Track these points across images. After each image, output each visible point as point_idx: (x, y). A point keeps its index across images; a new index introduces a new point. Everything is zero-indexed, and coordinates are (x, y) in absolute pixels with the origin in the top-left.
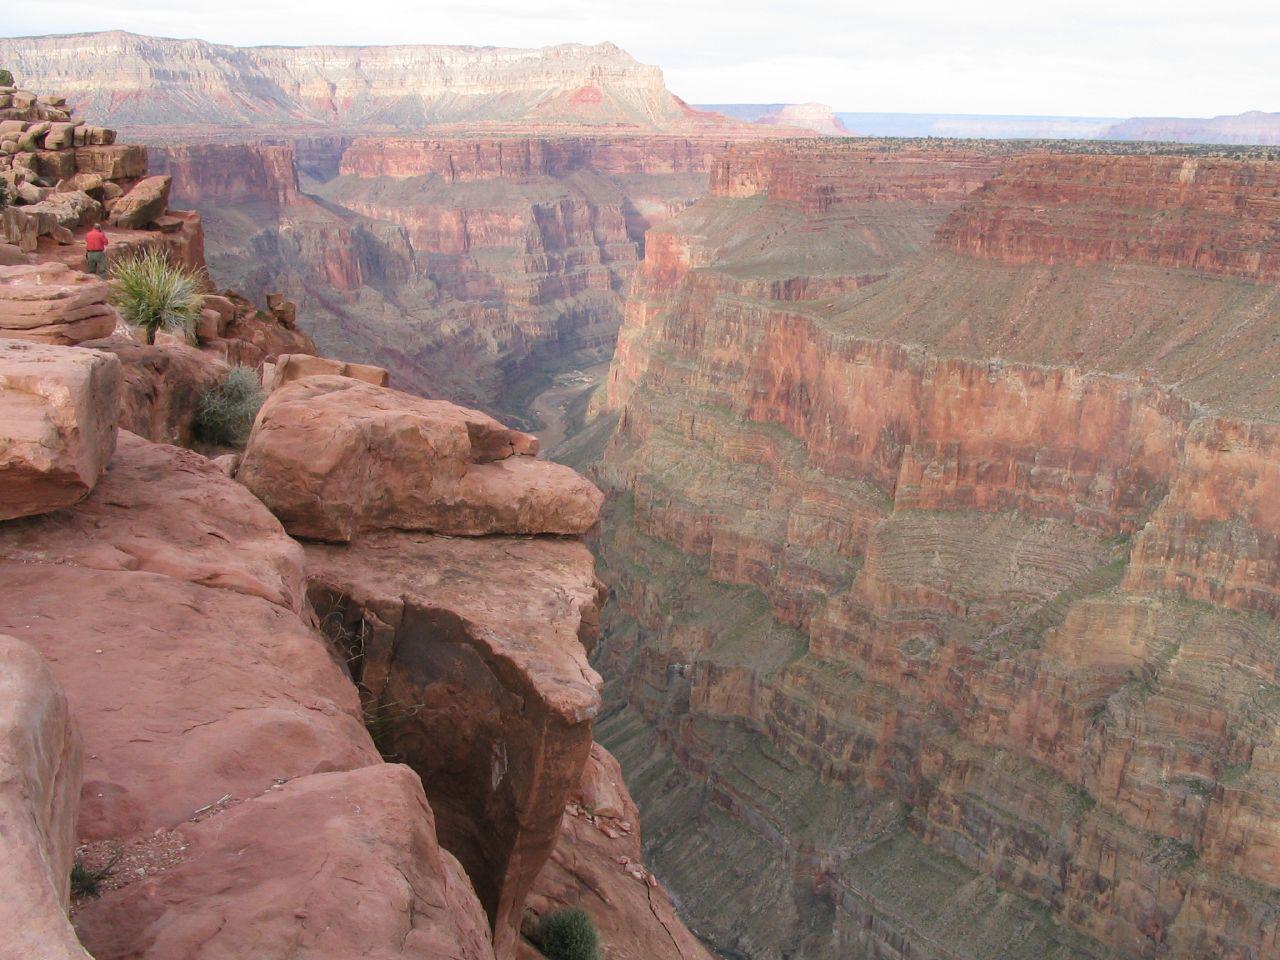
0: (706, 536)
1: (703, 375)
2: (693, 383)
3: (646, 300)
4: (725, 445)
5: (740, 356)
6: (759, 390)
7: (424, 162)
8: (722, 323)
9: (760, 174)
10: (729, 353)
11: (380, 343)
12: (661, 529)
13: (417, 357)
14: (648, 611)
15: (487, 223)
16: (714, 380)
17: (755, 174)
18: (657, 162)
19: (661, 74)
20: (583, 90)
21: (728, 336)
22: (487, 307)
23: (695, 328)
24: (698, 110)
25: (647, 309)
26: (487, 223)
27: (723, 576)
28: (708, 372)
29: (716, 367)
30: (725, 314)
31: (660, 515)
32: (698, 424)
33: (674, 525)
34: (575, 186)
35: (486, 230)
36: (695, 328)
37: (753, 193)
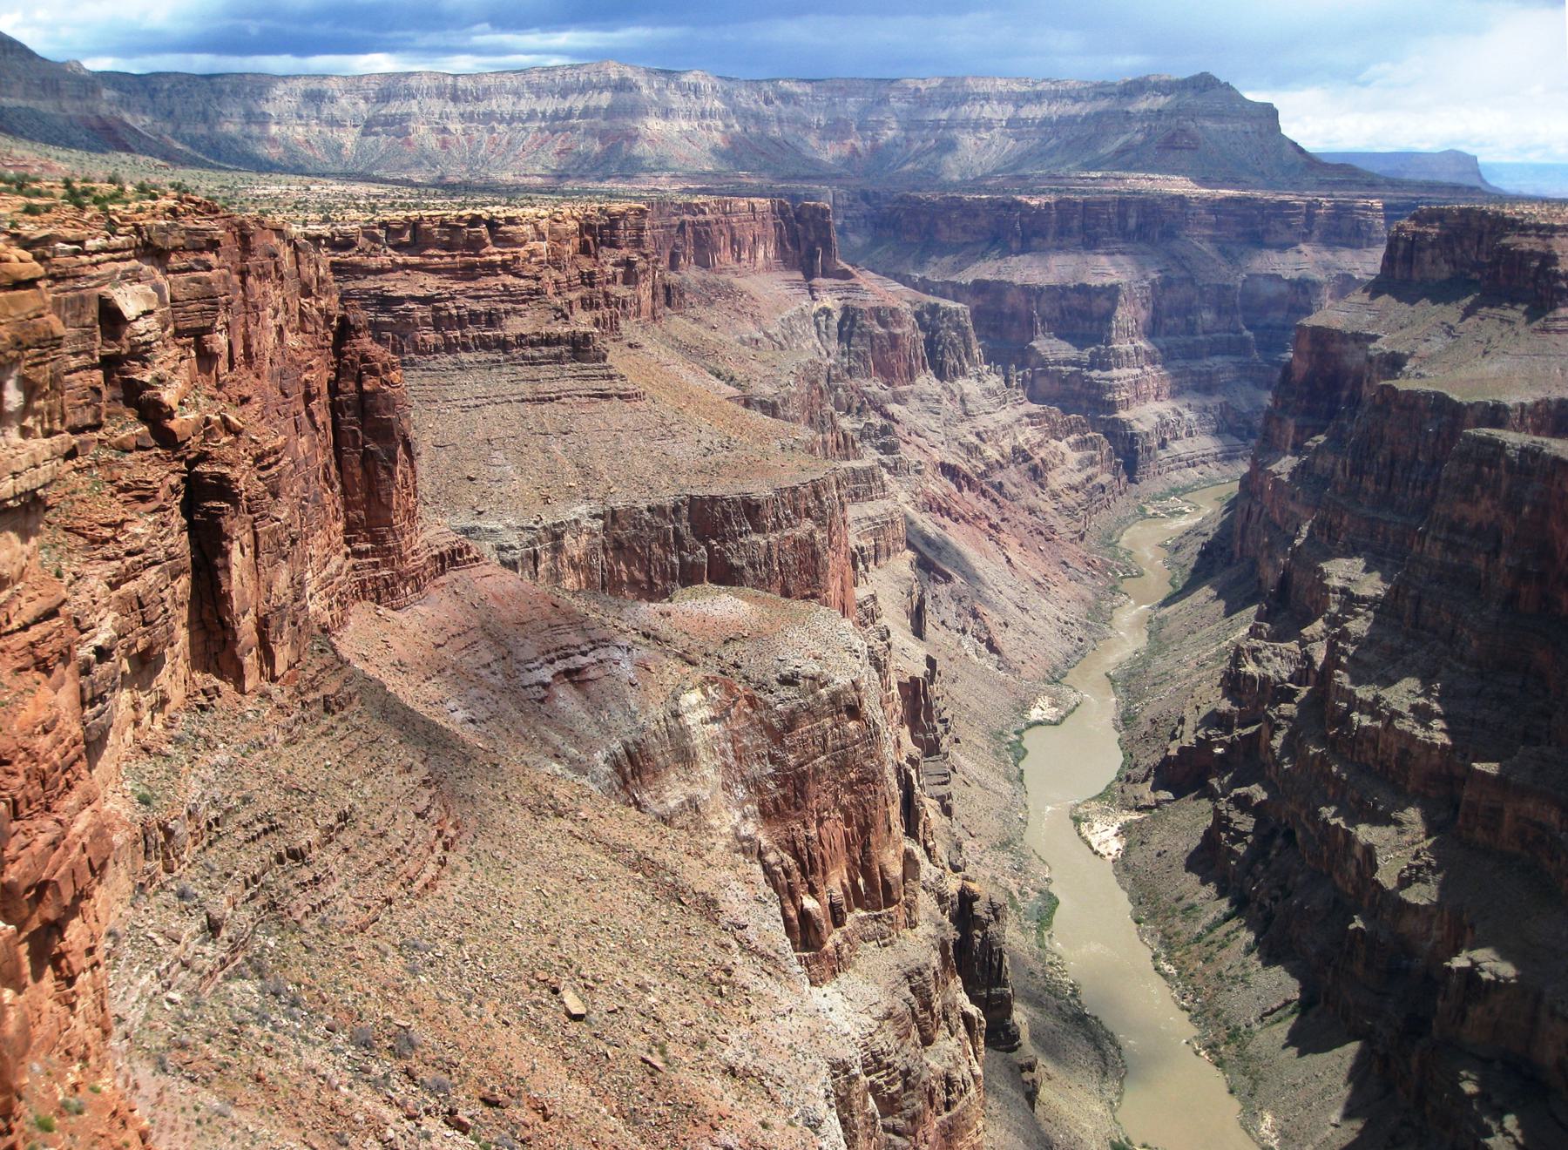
0: (1444, 771)
1: (1435, 539)
2: (1417, 548)
3: (1293, 415)
4: (1475, 643)
5: (1497, 516)
6: (1530, 568)
7: (984, 223)
8: (1471, 468)
9: (1458, 251)
10: (1483, 510)
11: (937, 458)
12: (1371, 754)
13: (979, 476)
14: (1353, 871)
15: (1064, 303)
16: (1449, 546)
17: (1452, 250)
18: (1279, 227)
19: (1275, 113)
20: (1174, 135)
21: (1477, 487)
22: (1066, 411)
23: (1393, 463)
24: (1377, 168)
25: (1297, 427)
26: (1064, 303)
27: (1479, 835)
28: (1443, 535)
29: (1454, 528)
30: (1474, 454)
31: (1372, 734)
32: (1426, 608)
33: (1395, 752)
34: (1175, 257)
35: (1062, 312)
36: (1393, 463)
37: (1445, 276)
